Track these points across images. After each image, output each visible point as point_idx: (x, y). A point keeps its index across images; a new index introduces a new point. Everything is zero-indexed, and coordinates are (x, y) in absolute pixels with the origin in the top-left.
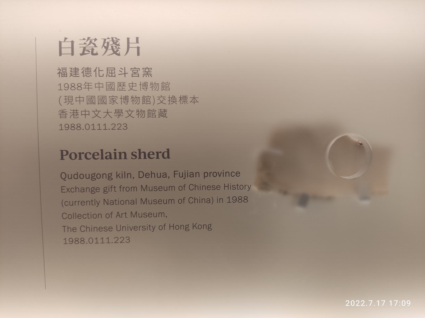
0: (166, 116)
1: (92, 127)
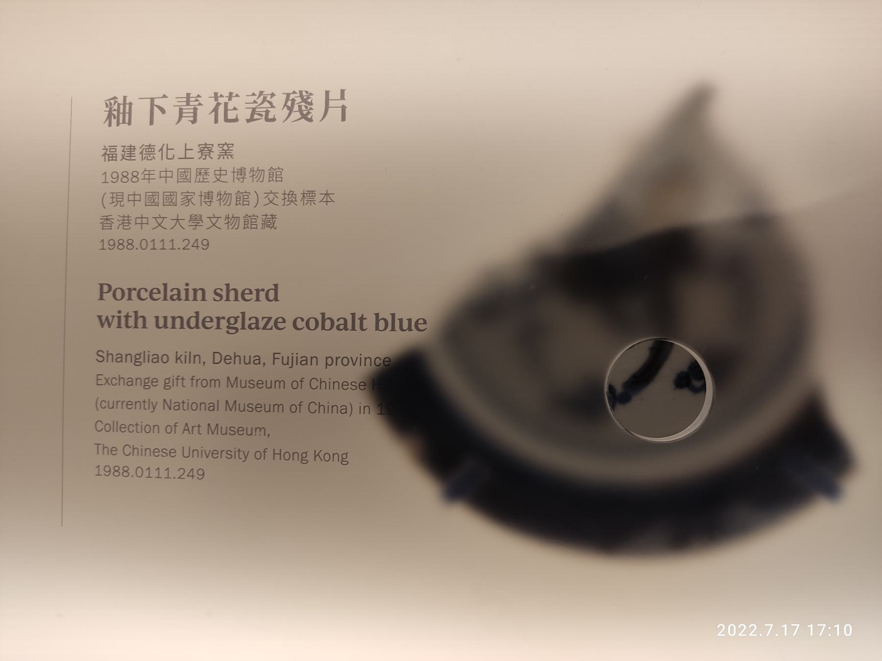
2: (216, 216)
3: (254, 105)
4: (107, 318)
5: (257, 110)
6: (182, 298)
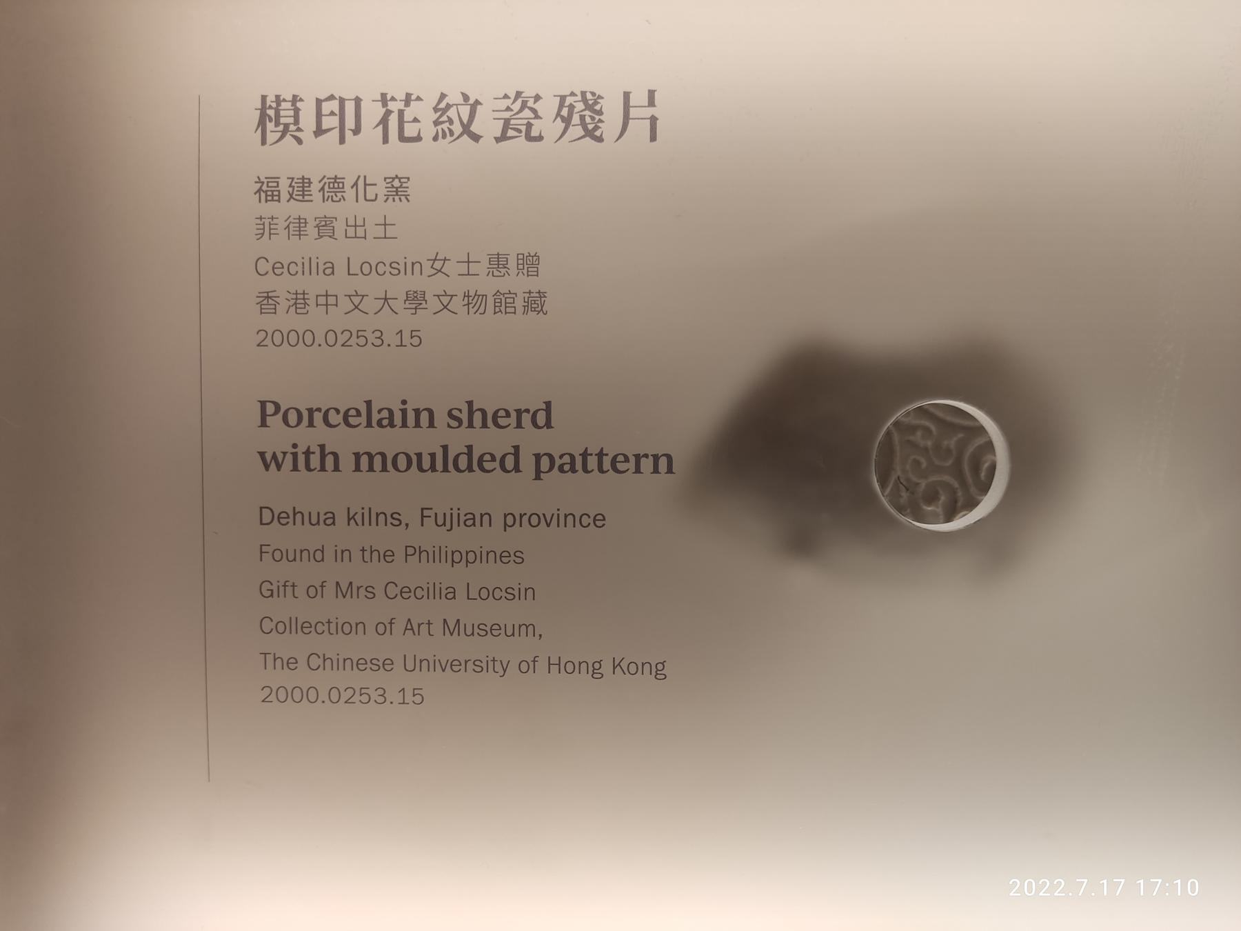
3: (507, 115)
4: (274, 456)
5: (512, 122)
6: (395, 423)
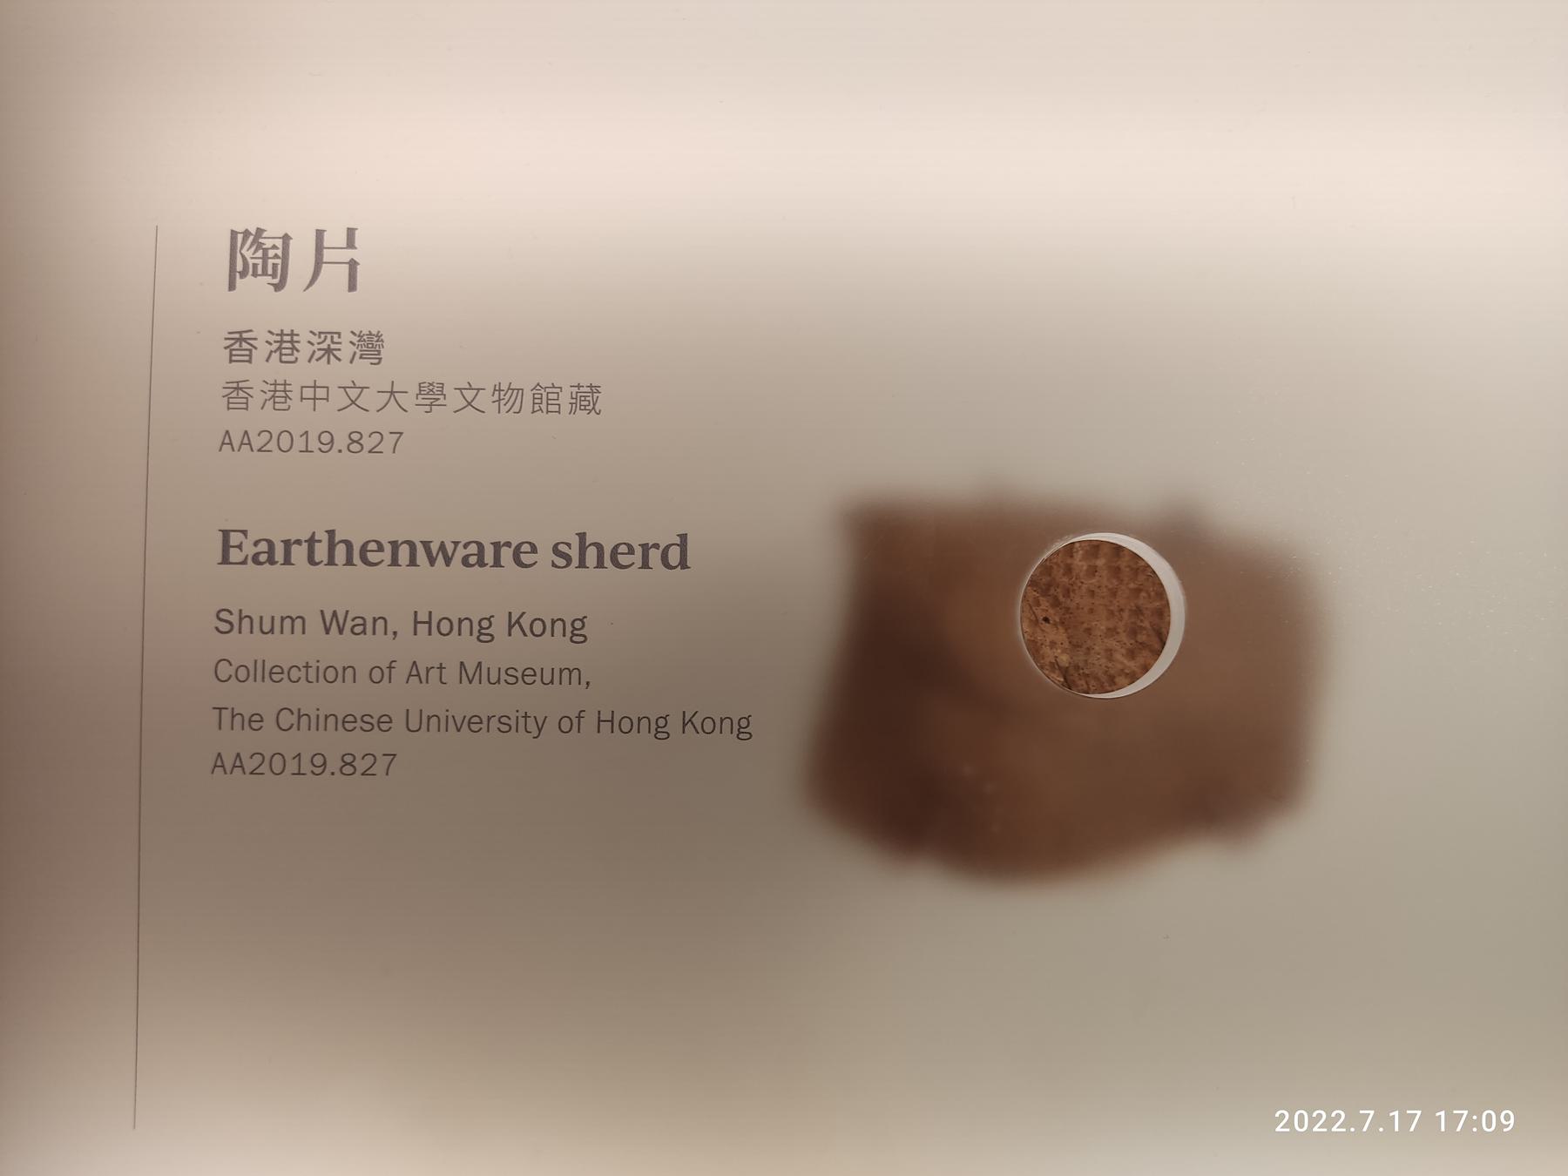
0: (596, 407)
1: (299, 443)
2: (473, 387)
